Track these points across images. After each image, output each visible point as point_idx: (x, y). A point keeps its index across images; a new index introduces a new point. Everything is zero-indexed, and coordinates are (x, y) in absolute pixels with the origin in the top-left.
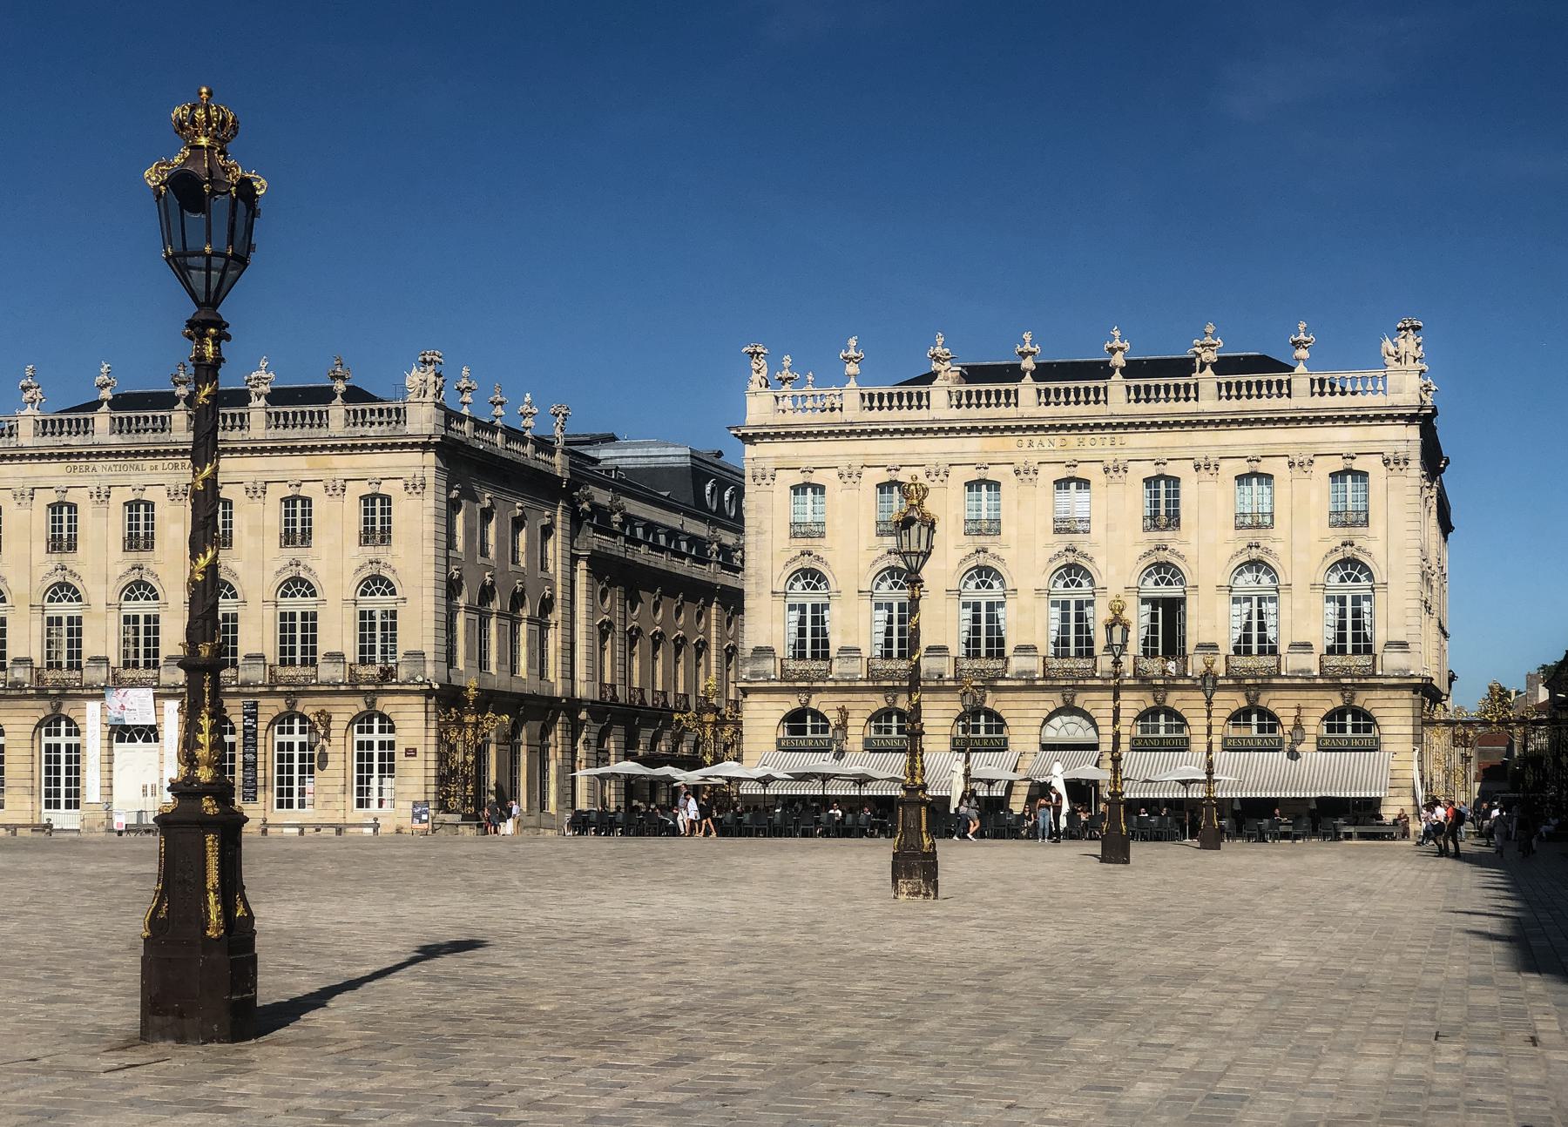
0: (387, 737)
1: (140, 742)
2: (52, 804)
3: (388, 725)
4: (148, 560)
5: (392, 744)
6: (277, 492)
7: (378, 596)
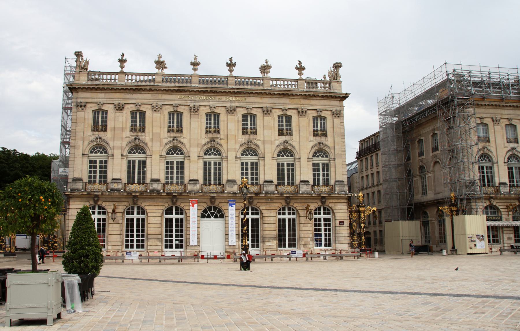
1: (212, 218)
2: (168, 246)
3: (327, 211)
4: (217, 138)
6: (276, 113)
7: (320, 157)
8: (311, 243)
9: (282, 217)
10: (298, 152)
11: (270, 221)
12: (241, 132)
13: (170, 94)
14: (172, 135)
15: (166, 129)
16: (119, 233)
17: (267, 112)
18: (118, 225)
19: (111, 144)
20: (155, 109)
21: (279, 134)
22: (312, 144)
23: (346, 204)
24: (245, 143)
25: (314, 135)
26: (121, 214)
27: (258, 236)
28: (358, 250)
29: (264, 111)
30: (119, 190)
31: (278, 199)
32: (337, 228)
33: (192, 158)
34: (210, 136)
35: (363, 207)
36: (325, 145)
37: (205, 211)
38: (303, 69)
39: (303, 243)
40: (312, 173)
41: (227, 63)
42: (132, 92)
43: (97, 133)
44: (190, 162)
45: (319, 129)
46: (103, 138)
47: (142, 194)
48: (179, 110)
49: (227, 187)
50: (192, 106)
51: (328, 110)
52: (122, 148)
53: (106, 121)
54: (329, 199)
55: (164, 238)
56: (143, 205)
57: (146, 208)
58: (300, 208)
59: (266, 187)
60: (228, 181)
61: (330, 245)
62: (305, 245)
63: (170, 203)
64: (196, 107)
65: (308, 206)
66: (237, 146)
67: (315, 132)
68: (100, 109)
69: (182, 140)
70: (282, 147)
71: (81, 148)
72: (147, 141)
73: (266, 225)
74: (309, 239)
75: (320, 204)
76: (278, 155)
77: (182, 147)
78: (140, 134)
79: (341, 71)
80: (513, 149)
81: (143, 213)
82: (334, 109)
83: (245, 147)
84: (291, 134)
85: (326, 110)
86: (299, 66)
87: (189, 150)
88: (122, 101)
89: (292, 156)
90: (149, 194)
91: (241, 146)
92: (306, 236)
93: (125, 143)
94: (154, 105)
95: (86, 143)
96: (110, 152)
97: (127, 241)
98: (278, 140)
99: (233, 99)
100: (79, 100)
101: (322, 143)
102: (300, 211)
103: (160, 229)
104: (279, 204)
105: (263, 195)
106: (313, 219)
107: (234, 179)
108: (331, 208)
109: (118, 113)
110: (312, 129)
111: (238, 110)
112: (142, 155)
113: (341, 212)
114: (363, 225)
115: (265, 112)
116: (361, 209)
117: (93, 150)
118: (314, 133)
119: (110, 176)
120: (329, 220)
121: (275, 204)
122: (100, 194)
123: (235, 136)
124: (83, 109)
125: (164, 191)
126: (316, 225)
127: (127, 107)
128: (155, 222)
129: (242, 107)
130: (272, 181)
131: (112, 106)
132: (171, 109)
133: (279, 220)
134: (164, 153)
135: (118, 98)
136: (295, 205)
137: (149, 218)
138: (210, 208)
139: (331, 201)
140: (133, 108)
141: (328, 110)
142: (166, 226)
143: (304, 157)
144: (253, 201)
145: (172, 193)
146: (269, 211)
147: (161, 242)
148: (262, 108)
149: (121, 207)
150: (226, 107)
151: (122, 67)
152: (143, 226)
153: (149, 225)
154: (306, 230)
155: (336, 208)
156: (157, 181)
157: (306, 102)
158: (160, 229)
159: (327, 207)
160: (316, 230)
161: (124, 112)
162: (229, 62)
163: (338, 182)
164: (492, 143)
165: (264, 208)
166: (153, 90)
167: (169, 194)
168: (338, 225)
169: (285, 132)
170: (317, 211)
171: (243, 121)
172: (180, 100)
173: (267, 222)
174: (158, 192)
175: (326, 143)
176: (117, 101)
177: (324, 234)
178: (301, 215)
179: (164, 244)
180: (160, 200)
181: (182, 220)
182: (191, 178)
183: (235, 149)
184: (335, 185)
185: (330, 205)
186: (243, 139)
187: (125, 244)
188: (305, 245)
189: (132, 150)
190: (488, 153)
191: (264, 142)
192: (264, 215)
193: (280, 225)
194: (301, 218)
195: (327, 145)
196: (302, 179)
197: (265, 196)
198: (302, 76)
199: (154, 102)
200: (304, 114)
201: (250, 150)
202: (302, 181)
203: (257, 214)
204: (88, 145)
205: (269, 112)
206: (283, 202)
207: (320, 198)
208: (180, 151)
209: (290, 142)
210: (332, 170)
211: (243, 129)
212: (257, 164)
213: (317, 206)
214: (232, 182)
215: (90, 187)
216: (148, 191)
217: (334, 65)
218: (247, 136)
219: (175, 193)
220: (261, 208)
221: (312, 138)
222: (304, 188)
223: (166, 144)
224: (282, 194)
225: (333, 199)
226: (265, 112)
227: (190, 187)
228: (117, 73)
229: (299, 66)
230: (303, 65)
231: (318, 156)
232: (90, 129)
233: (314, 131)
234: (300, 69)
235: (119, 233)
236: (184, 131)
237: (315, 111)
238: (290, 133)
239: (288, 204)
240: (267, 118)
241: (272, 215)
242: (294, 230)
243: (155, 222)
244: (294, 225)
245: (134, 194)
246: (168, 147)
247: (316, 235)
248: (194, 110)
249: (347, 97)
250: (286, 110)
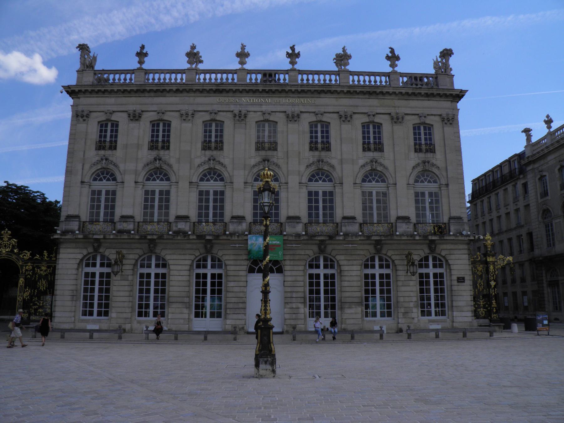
6: (359, 120)
7: (426, 183)
8: (415, 310)
9: (369, 271)
10: (393, 175)
11: (351, 277)
12: (307, 147)
13: (205, 96)
14: (208, 153)
15: (199, 146)
16: (127, 294)
17: (345, 118)
18: (126, 283)
19: (122, 167)
20: (184, 117)
21: (364, 150)
22: (412, 163)
23: (466, 252)
24: (313, 163)
25: (416, 151)
26: (131, 267)
27: (333, 299)
28: (486, 321)
29: (341, 117)
30: (128, 232)
31: (364, 244)
32: (455, 288)
33: (235, 185)
34: (263, 153)
35: (493, 256)
36: (433, 165)
38: (398, 58)
39: (402, 310)
40: (414, 205)
41: (288, 53)
42: (152, 94)
43: (102, 152)
44: (233, 191)
45: (423, 142)
46: (111, 158)
47: (161, 237)
48: (218, 118)
49: (287, 227)
50: (237, 112)
51: (435, 115)
52: (136, 173)
53: (116, 136)
54: (440, 244)
55: (194, 303)
56: (163, 254)
57: (168, 257)
58: (398, 257)
59: (345, 226)
60: (289, 218)
61: (443, 314)
62: (406, 313)
63: (203, 251)
64: (243, 113)
65: (410, 254)
66: (303, 168)
67: (417, 147)
68: (108, 120)
69: (222, 160)
70: (368, 168)
71: (80, 173)
72: (172, 161)
73: (346, 284)
74: (412, 305)
75: (427, 251)
76: (364, 181)
77: (223, 169)
78: (162, 152)
79: (453, 61)
81: (164, 266)
82: (444, 113)
83: (313, 168)
84: (381, 150)
85: (432, 115)
86: (390, 55)
87: (231, 174)
88: (138, 108)
89: (383, 181)
90: (171, 237)
91: (307, 166)
92: (407, 299)
93: (140, 166)
94: (183, 112)
95: (87, 167)
96: (119, 179)
97: (140, 306)
98: (363, 158)
99: (297, 101)
100: (80, 108)
101: (428, 162)
102: (397, 262)
103: (187, 289)
104: (367, 250)
105: (341, 238)
106: (417, 275)
107: (297, 214)
108: (444, 257)
109: (133, 125)
110: (412, 142)
111: (303, 116)
112: (165, 183)
113: (460, 263)
114: (493, 283)
115: (343, 119)
116: (490, 259)
117: (97, 177)
118: (415, 148)
119: (119, 212)
120: (441, 275)
121: (358, 252)
122: (102, 237)
123: (299, 153)
124: (84, 120)
125: (194, 233)
126: (421, 283)
127: (145, 115)
128: (180, 278)
129: (309, 112)
130: (353, 218)
131: (125, 115)
132: (207, 117)
133: (366, 276)
134: (195, 179)
135: (133, 103)
136: (390, 252)
137: (172, 273)
139: (445, 246)
140: (153, 116)
141: (435, 115)
142: (198, 284)
143: (402, 183)
144: (325, 247)
145: (205, 236)
146: (351, 263)
147: (189, 308)
148: (338, 113)
149: (131, 256)
150: (285, 112)
151: (141, 62)
152: (164, 284)
153: (172, 283)
155: (452, 257)
156: (185, 218)
158: (187, 289)
159: (438, 256)
160: (422, 291)
161: (141, 123)
162: (290, 52)
163: (454, 218)
165: (342, 257)
166: (182, 92)
167: (200, 237)
168: (455, 283)
169: (372, 146)
170: (423, 262)
171: (311, 132)
173: (347, 278)
174: (185, 233)
175: (434, 162)
176: (131, 108)
177: (433, 297)
178: (399, 268)
179: (194, 311)
180: (189, 246)
181: (220, 276)
182: (235, 214)
183: (299, 171)
184: (449, 223)
185: (443, 253)
186: (310, 156)
187: (137, 310)
188: (406, 313)
189: (152, 175)
191: (341, 162)
192: (343, 268)
193: (367, 284)
194: (399, 273)
195: (435, 165)
196: (400, 215)
197: (344, 240)
198: (396, 69)
199: (184, 108)
200: (400, 120)
201: (320, 173)
202: (398, 218)
203: (332, 267)
204: (91, 167)
205: (349, 119)
206: (371, 248)
207: (428, 242)
208: (219, 175)
209: (381, 160)
210: (444, 201)
211: (311, 142)
212: (331, 194)
213: (423, 255)
214: (294, 219)
215: (90, 227)
216: (170, 233)
217: (441, 53)
218: (317, 153)
219: (210, 235)
220: (338, 257)
221: (413, 155)
222: (402, 228)
223: (199, 166)
224: (369, 237)
225: (446, 244)
226: (343, 119)
227: (232, 228)
228: (132, 72)
229: (390, 55)
230: (396, 54)
231: (422, 182)
232: (94, 147)
233: (415, 144)
234: (393, 58)
235: (127, 294)
236: (225, 147)
237: (416, 116)
238: (379, 147)
239: (378, 251)
240: (346, 127)
241: (355, 268)
242: (389, 291)
243: (180, 278)
244: (388, 284)
245: (149, 237)
246: (201, 169)
247: (422, 299)
248: (240, 117)
249: (463, 96)
250: (374, 116)
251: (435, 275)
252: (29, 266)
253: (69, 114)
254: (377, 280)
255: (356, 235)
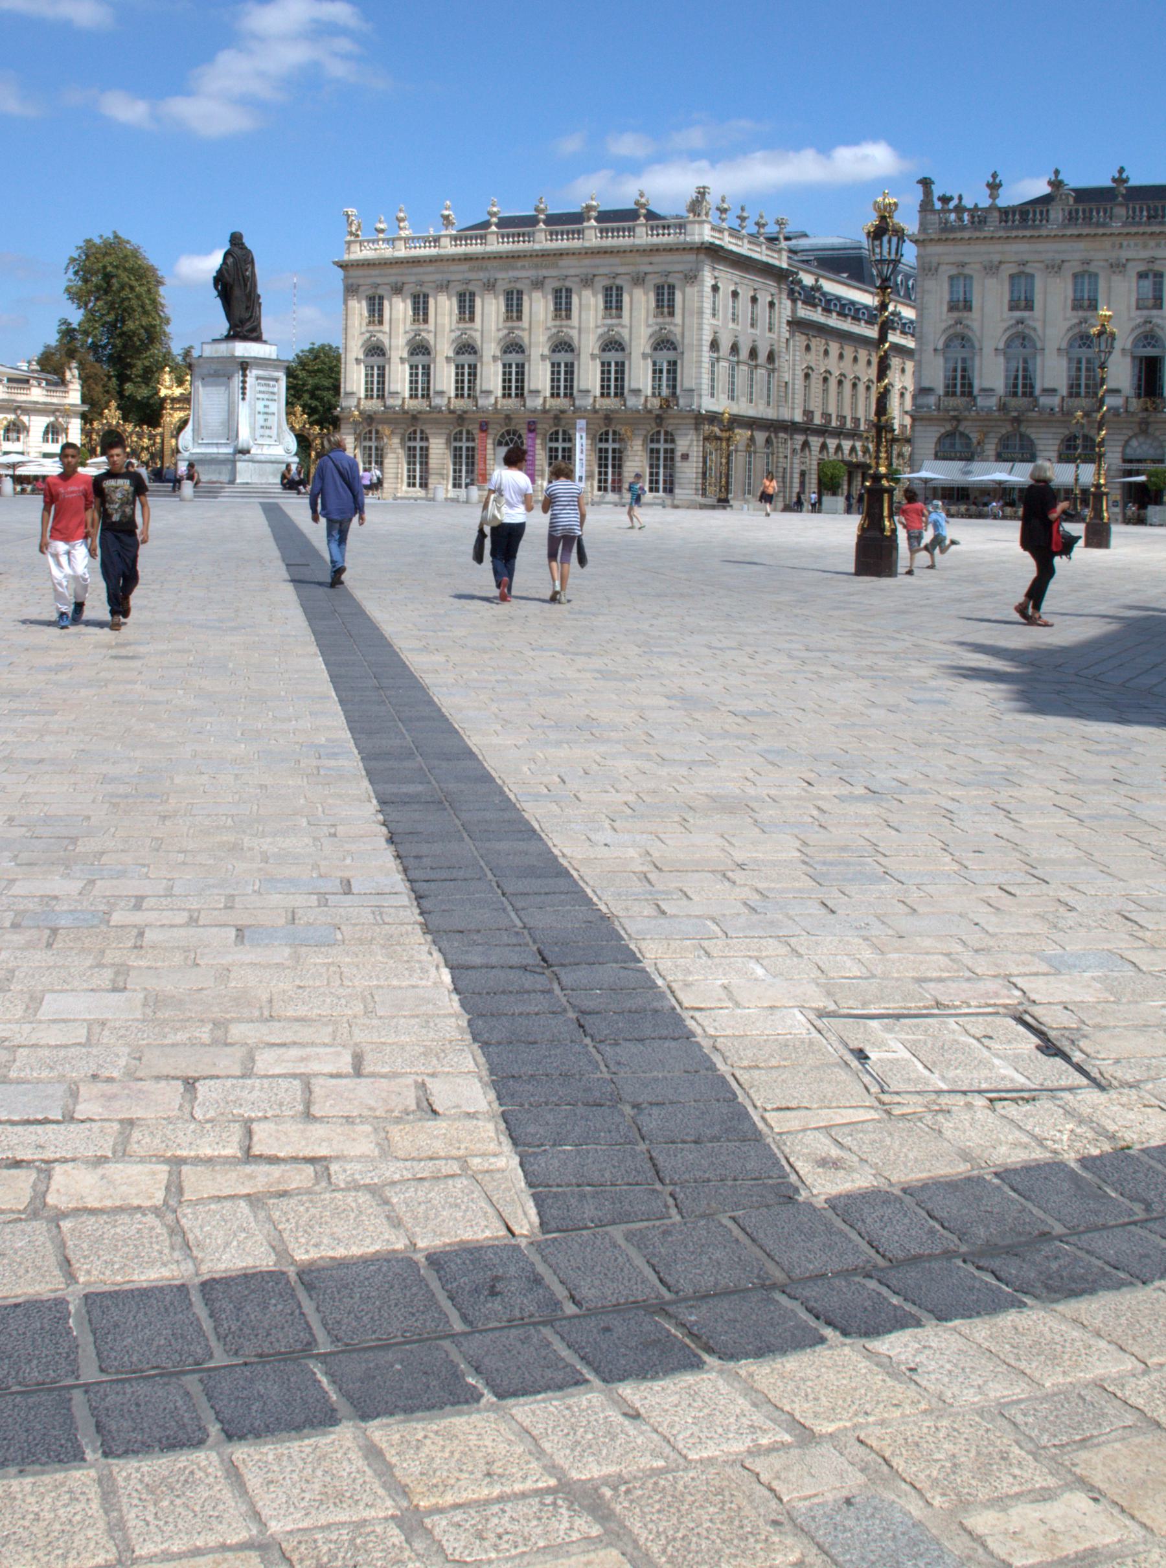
0: (669, 446)
5: (672, 451)
37: (502, 436)
80: (1021, 321)
100: (350, 281)
127: (406, 287)
138: (508, 433)
154: (636, 462)
157: (646, 259)
164: (975, 314)
172: (471, 270)
190: (966, 331)
221: (651, 320)
222: (632, 402)
251: (666, 451)
252: (318, 441)
253: (340, 286)
254: (610, 455)
255: (586, 410)
